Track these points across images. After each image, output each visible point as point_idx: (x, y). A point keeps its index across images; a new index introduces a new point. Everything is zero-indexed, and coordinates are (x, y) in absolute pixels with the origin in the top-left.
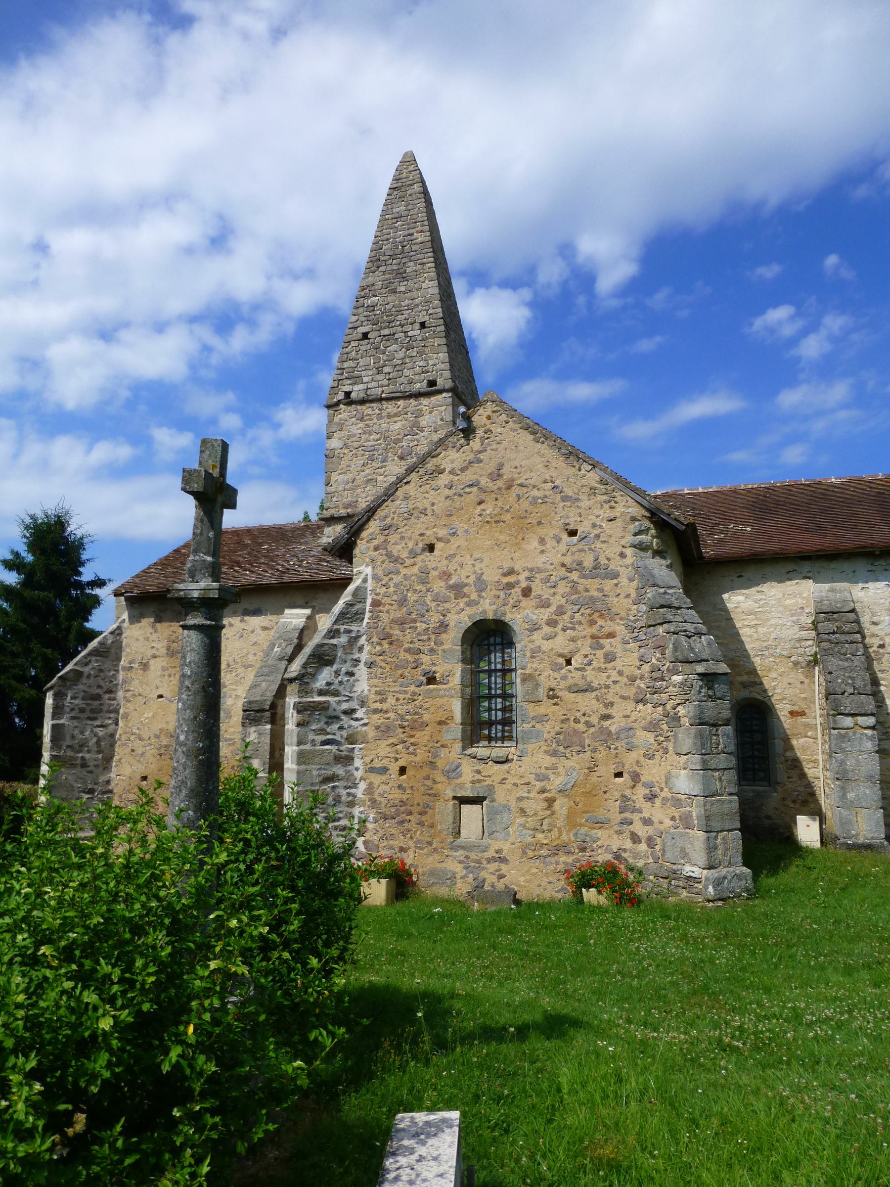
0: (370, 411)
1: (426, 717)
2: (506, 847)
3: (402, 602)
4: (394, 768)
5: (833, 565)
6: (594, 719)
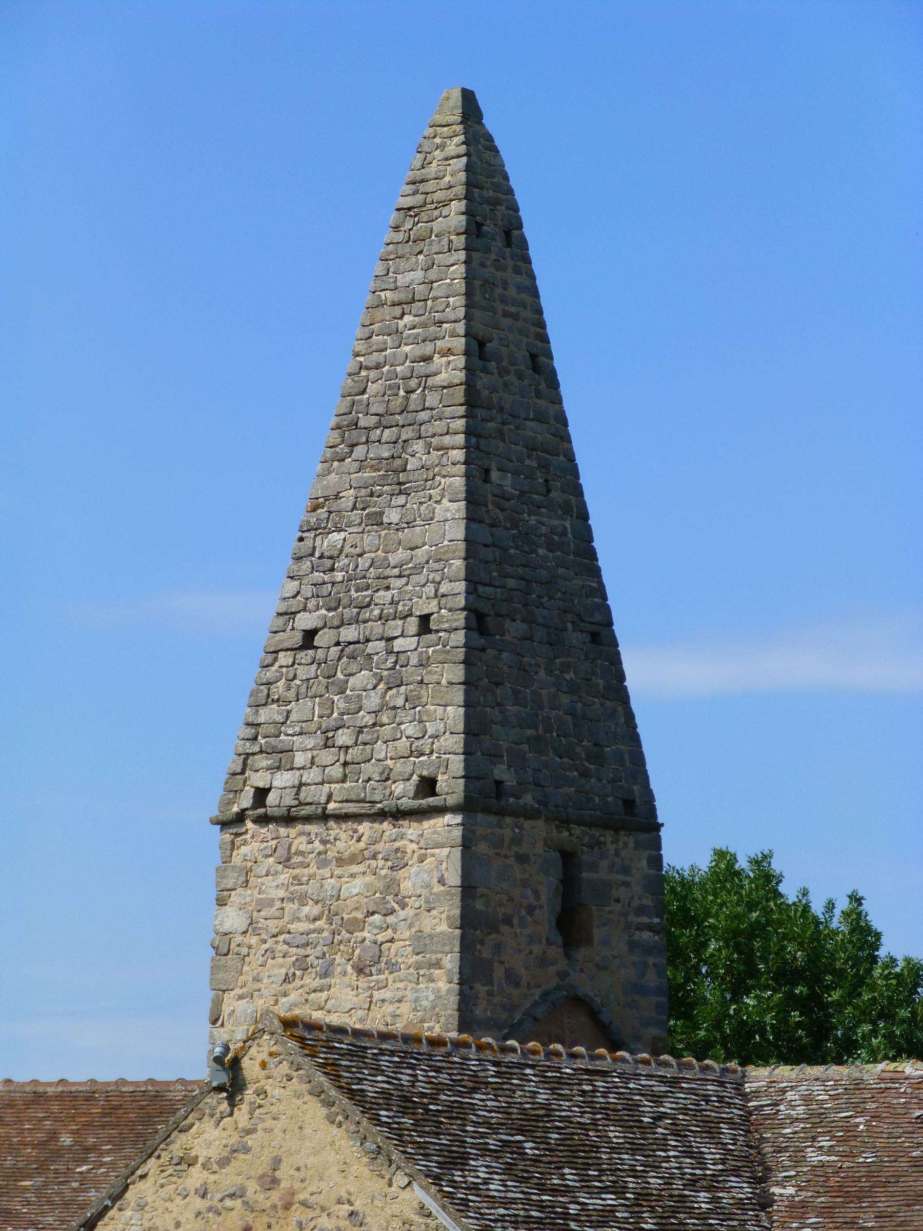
0: (300, 844)
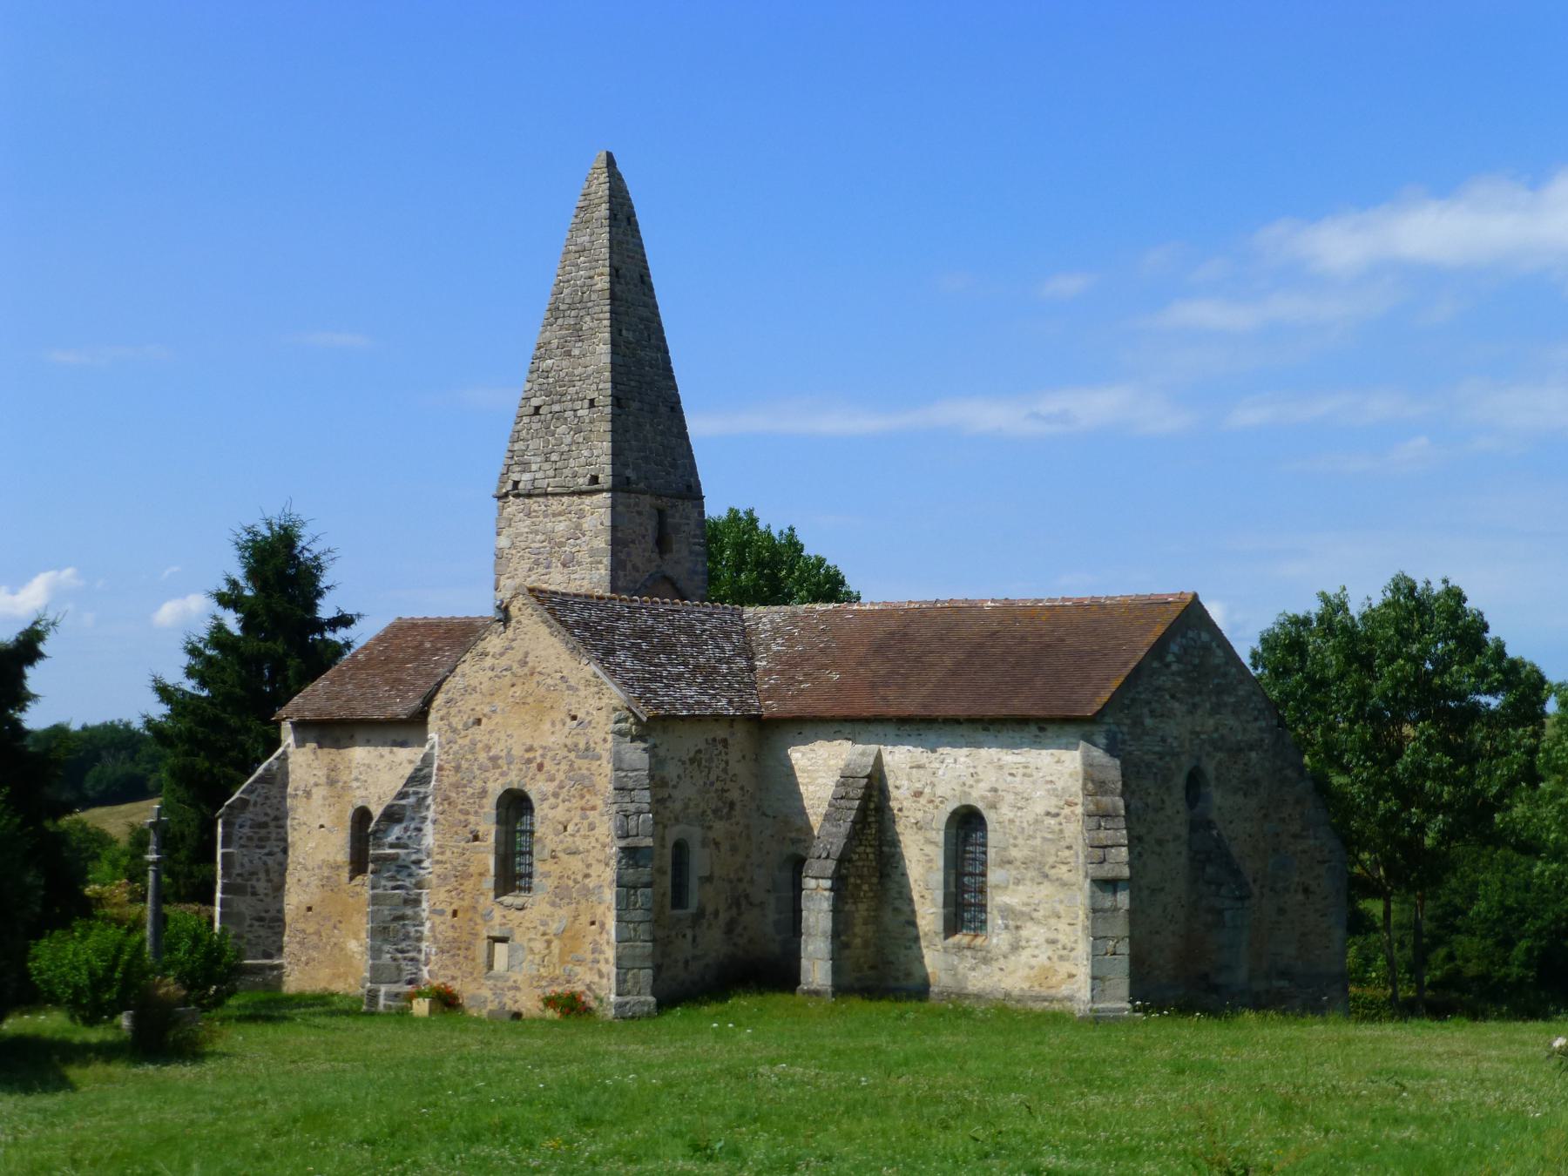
0: (535, 507)
1: (472, 869)
2: (519, 978)
3: (457, 769)
4: (449, 911)
5: (871, 728)
6: (579, 878)
